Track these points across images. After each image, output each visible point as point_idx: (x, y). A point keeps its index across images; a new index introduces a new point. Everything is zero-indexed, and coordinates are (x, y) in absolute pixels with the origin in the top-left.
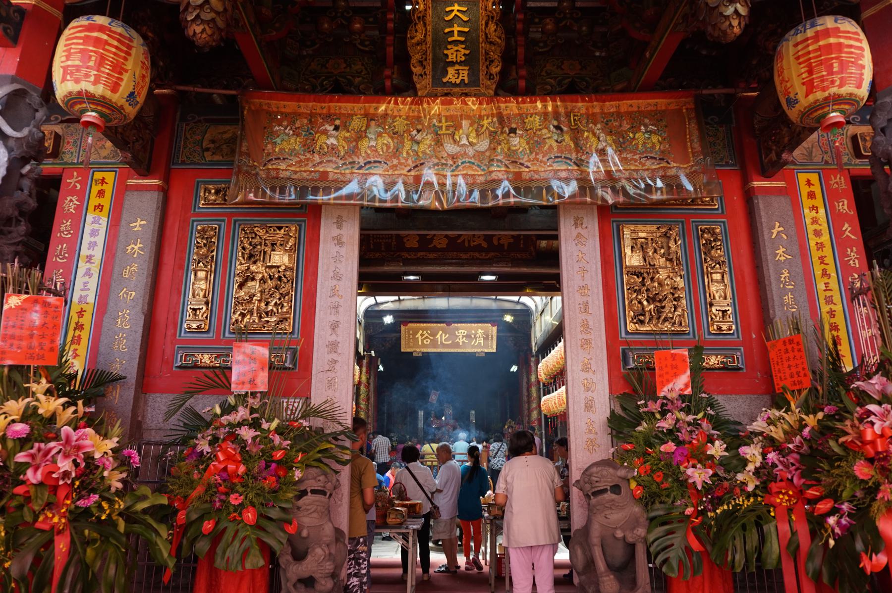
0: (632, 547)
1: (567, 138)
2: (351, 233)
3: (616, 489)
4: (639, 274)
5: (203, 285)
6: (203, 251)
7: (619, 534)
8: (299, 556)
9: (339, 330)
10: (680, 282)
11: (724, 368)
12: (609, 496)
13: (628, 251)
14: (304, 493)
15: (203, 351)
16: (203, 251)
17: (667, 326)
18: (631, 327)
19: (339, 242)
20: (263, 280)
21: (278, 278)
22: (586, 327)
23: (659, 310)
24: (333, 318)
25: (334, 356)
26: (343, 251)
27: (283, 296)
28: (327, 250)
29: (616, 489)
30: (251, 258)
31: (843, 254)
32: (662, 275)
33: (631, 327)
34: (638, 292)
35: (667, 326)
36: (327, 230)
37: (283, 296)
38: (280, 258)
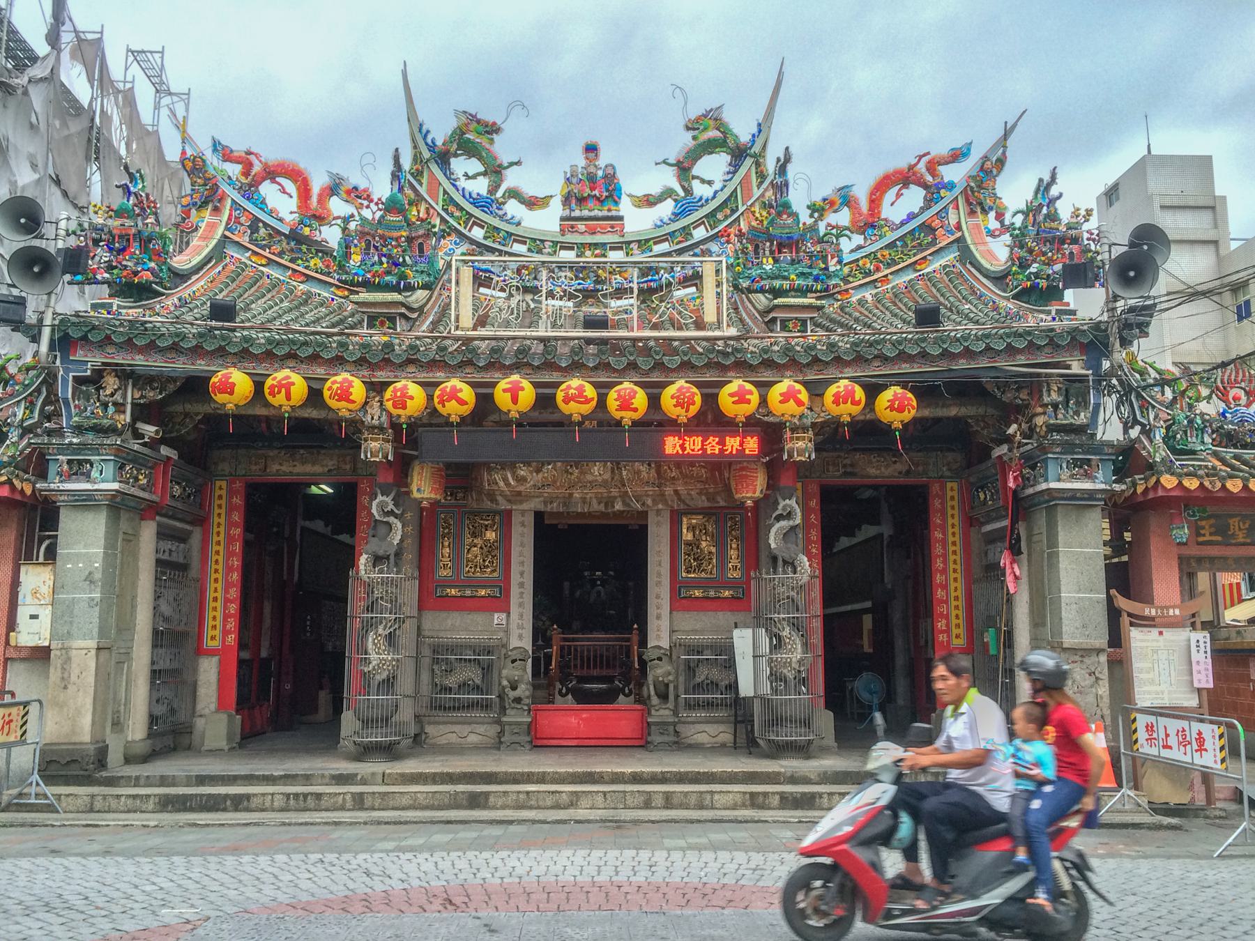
0: (667, 685)
1: (653, 471)
2: (530, 520)
3: (660, 659)
4: (690, 545)
5: (448, 550)
6: (446, 531)
7: (661, 679)
8: (514, 688)
9: (525, 575)
10: (713, 550)
11: (733, 597)
12: (656, 662)
13: (685, 531)
14: (515, 660)
15: (451, 587)
16: (446, 531)
17: (703, 575)
18: (684, 575)
19: (523, 524)
20: (481, 548)
21: (489, 549)
22: (659, 575)
23: (699, 566)
24: (521, 568)
25: (522, 590)
26: (525, 530)
27: (493, 557)
28: (516, 531)
29: (660, 659)
30: (474, 535)
31: (808, 533)
32: (704, 544)
33: (684, 575)
34: (689, 555)
35: (703, 575)
36: (516, 519)
37: (493, 557)
38: (491, 535)
